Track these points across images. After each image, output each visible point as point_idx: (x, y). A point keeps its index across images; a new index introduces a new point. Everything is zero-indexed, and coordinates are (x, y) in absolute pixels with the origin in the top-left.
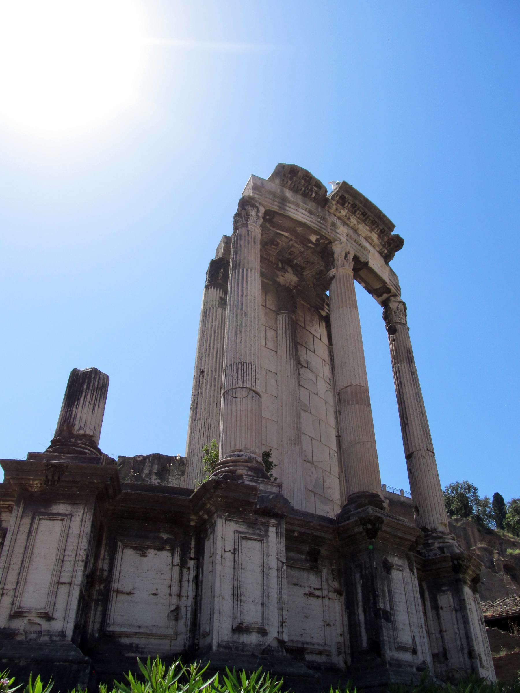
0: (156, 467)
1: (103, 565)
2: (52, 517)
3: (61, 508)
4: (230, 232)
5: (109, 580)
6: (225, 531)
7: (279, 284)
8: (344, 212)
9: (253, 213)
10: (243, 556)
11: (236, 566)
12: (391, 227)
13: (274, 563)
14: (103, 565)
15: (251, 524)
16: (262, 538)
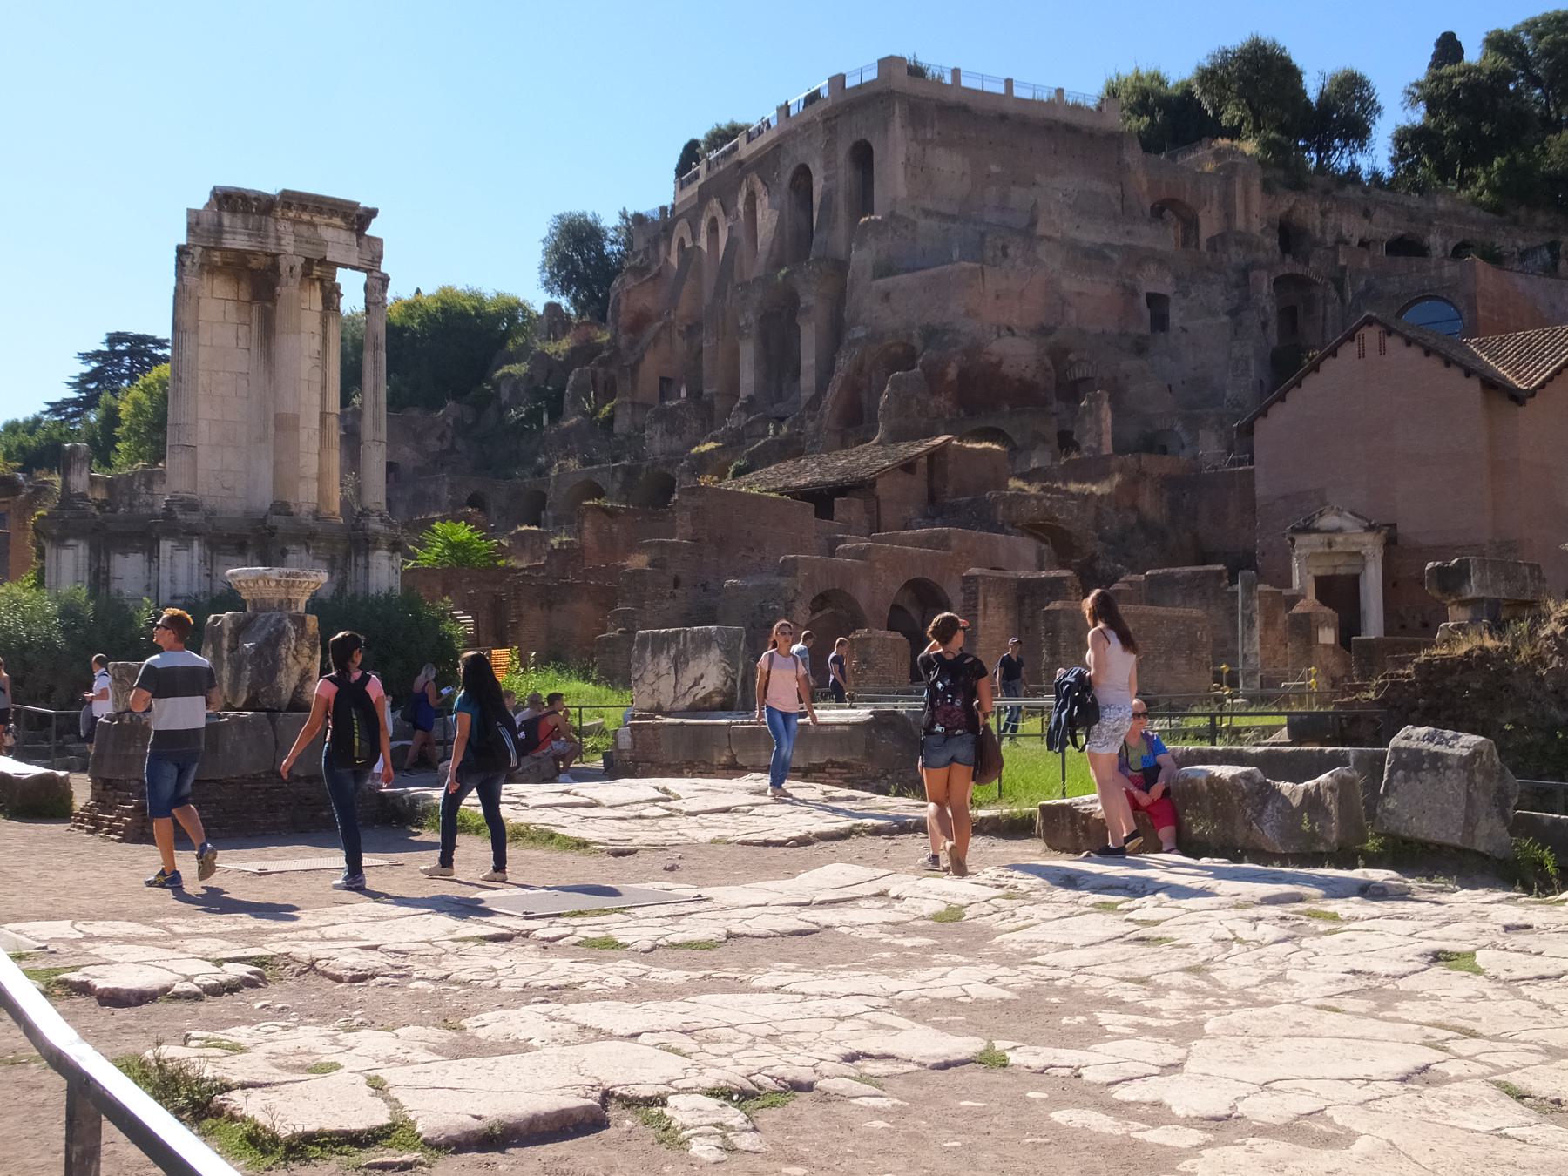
0: (143, 481)
1: (103, 564)
2: (67, 547)
3: (71, 542)
4: (183, 241)
5: (108, 572)
6: (166, 546)
7: (252, 270)
8: (291, 215)
9: (188, 263)
10: (176, 559)
11: (173, 565)
12: (355, 205)
13: (196, 561)
14: (103, 564)
15: (180, 541)
16: (188, 547)
